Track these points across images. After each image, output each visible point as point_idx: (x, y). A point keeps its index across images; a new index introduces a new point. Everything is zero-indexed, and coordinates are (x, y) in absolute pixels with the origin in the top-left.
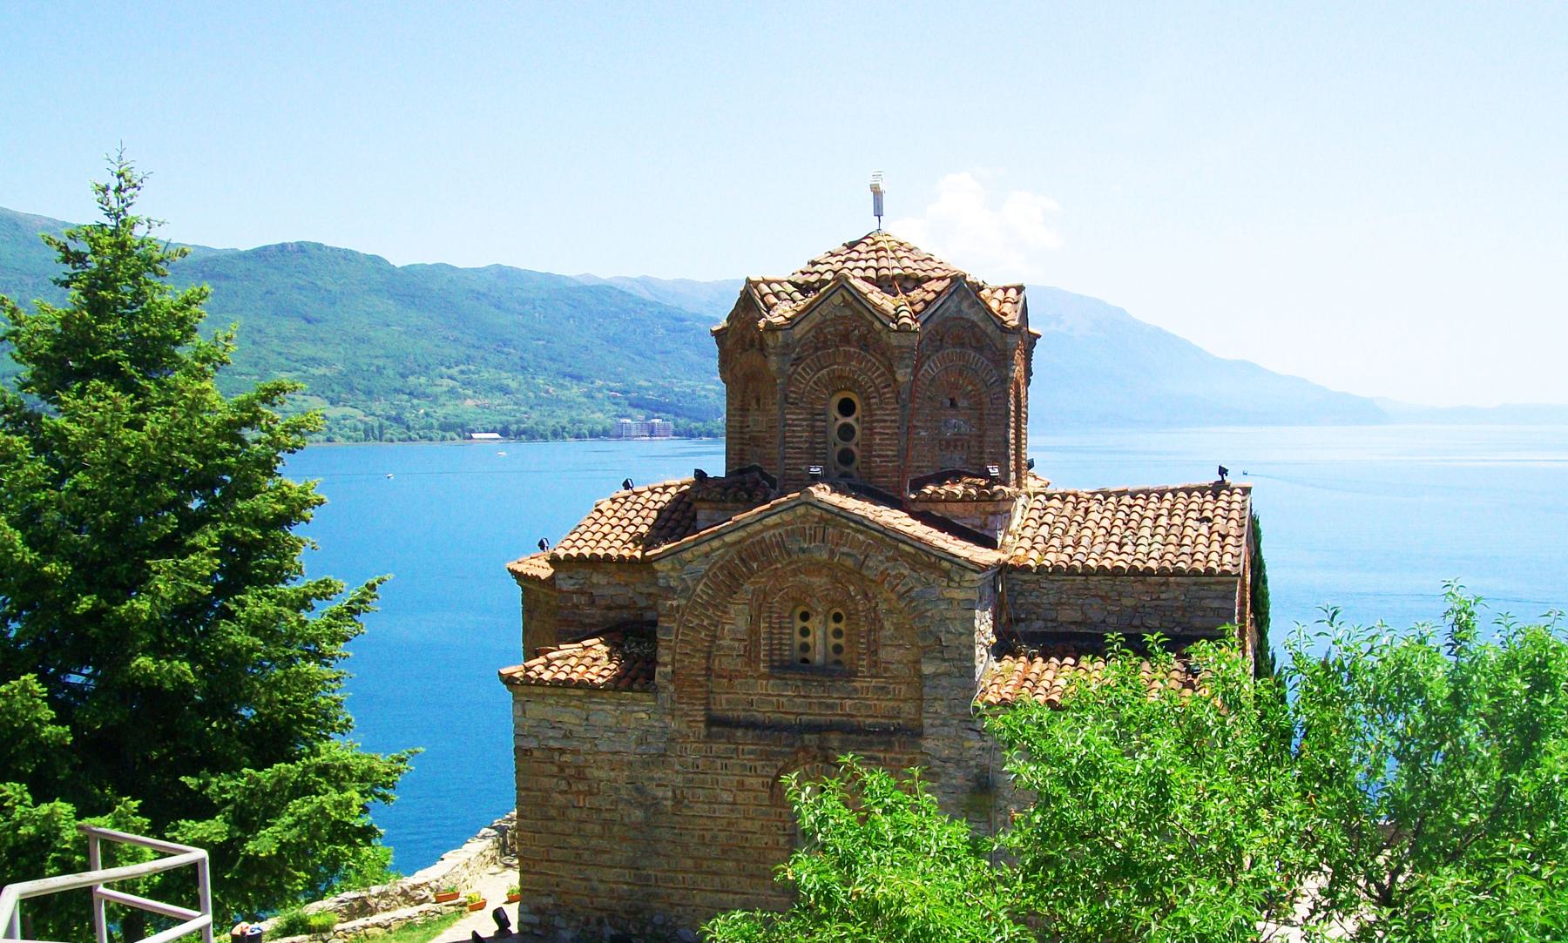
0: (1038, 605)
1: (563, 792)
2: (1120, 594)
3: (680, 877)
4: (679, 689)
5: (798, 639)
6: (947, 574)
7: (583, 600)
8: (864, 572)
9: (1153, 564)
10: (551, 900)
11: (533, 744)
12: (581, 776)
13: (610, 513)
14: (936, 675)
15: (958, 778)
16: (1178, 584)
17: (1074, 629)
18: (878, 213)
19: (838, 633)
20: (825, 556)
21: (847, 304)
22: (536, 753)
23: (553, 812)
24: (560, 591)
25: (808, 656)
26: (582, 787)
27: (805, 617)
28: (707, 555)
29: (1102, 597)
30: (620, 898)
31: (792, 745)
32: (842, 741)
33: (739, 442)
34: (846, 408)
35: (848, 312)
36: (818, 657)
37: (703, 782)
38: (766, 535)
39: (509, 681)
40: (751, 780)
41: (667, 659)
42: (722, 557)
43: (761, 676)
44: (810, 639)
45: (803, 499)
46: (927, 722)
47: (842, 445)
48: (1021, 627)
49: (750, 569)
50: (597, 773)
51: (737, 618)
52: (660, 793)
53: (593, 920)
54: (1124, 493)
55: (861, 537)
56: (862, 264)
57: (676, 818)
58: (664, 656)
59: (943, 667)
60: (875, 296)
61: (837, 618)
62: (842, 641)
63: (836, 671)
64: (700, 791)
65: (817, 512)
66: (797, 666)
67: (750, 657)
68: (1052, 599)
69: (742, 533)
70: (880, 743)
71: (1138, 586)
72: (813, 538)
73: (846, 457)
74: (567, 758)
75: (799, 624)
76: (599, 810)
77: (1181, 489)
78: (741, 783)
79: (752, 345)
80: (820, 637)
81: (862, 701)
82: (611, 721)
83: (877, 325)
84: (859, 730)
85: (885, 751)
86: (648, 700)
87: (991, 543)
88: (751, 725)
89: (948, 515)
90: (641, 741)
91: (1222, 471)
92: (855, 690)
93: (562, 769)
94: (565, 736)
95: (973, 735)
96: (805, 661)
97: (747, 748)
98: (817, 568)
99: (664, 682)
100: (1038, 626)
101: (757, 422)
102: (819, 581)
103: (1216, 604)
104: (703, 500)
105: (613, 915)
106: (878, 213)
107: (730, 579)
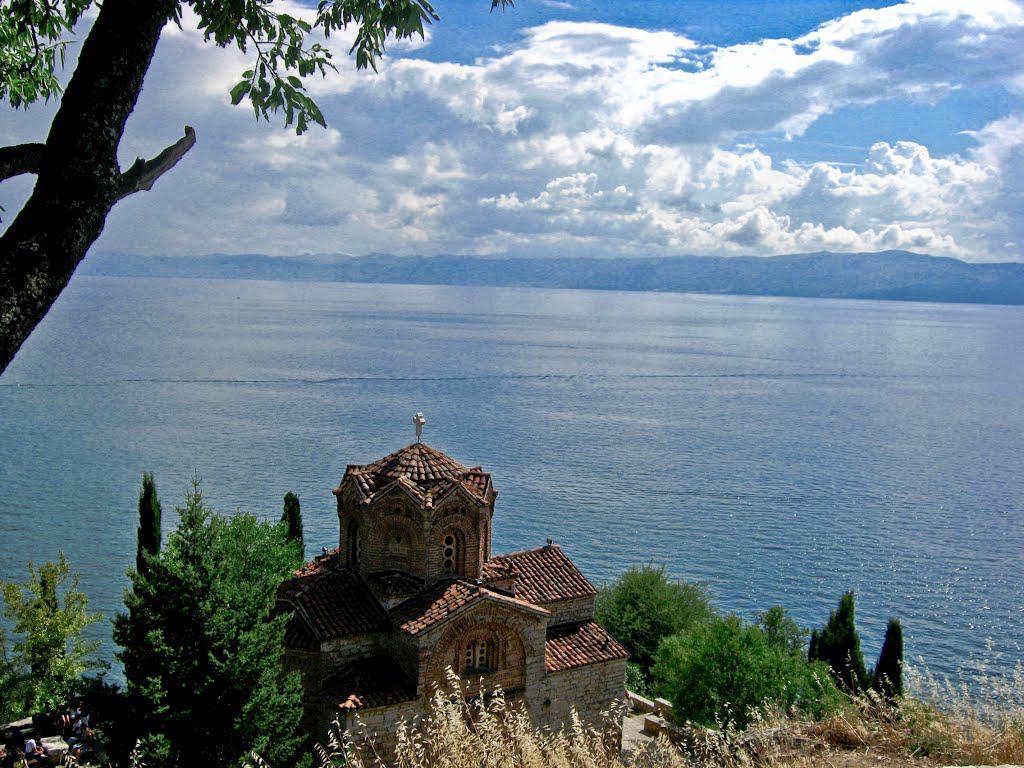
6: (538, 620)
18: (418, 433)
25: (471, 664)
27: (469, 647)
28: (441, 629)
59: (534, 659)
61: (483, 645)
83: (471, 504)
86: (415, 703)
103: (588, 607)
106: (418, 433)
107: (450, 637)
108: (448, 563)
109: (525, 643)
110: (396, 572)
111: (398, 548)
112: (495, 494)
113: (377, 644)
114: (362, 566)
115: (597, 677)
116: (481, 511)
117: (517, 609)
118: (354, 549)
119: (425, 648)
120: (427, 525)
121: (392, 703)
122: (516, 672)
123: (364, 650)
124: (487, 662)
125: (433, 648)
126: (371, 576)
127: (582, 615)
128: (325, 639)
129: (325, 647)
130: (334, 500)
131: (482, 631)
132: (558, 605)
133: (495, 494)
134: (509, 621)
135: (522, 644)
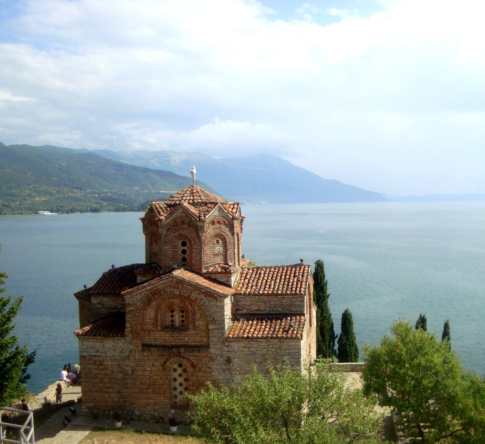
0: (245, 305)
1: (96, 369)
2: (270, 301)
3: (134, 395)
4: (133, 335)
5: (170, 319)
6: (216, 298)
7: (100, 306)
8: (191, 298)
9: (280, 292)
10: (92, 404)
11: (86, 354)
13: (107, 277)
14: (213, 329)
15: (221, 360)
16: (287, 298)
17: (256, 312)
19: (183, 316)
20: (178, 293)
21: (183, 212)
22: (87, 357)
23: (92, 376)
24: (93, 304)
25: (174, 323)
26: (102, 367)
27: (172, 311)
28: (141, 293)
29: (264, 302)
30: (115, 403)
31: (169, 352)
32: (185, 351)
33: (150, 253)
34: (184, 244)
35: (184, 215)
36: (177, 323)
37: (141, 364)
38: (160, 287)
39: (78, 335)
40: (157, 363)
41: (129, 326)
42: (145, 294)
43: (159, 331)
44: (174, 318)
45: (171, 276)
46: (211, 344)
47: (183, 256)
48: (240, 312)
49: (155, 297)
51: (150, 313)
52: (127, 368)
53: (106, 410)
54: (271, 267)
55: (189, 287)
56: (188, 198)
57: (133, 376)
58: (128, 325)
60: (192, 209)
61: (182, 312)
62: (184, 319)
64: (140, 368)
65: (175, 280)
66: (171, 328)
67: (155, 324)
68: (249, 303)
69: (152, 286)
70: (197, 351)
71: (275, 299)
72: (174, 288)
73: (184, 259)
74: (97, 358)
75: (170, 314)
76: (107, 374)
77: (290, 266)
78: (153, 365)
79: (153, 224)
80: (177, 318)
81: (190, 337)
82: (111, 346)
83: (193, 219)
85: (199, 353)
87: (229, 286)
88: (156, 346)
89: (216, 278)
90: (121, 352)
91: (302, 260)
92: (188, 334)
93: (95, 362)
94: (96, 352)
95: (226, 347)
96: (172, 325)
97: (155, 353)
98: (175, 297)
99: (128, 334)
100: (245, 311)
101: (155, 248)
102: (176, 301)
103: (299, 303)
104: (138, 274)
107: (148, 301)
109: (207, 314)
110: (154, 263)
115: (273, 350)
117: (197, 287)
119: (130, 304)
122: (204, 334)
127: (293, 309)
131: (175, 301)
134: (192, 295)
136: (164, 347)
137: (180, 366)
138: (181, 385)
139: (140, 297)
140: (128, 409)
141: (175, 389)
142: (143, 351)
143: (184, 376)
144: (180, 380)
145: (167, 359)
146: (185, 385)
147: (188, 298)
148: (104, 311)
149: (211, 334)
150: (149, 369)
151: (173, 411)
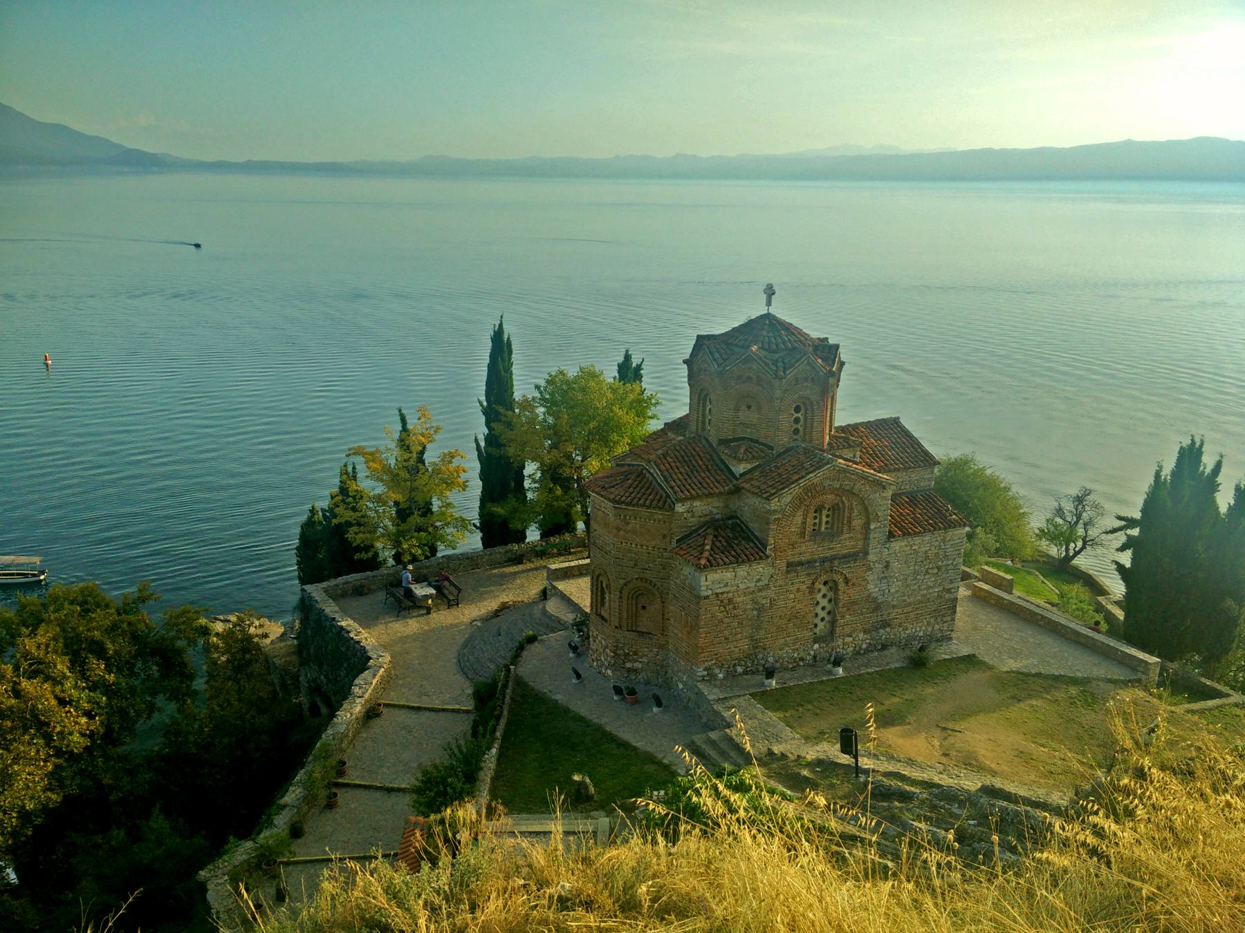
12: (730, 601)
15: (879, 567)
18: (769, 303)
21: (809, 364)
34: (797, 410)
47: (795, 426)
50: (739, 600)
58: (771, 541)
63: (833, 534)
67: (802, 534)
84: (844, 556)
88: (801, 564)
90: (759, 580)
98: (833, 491)
105: (739, 660)
106: (769, 303)
108: (796, 431)
109: (870, 510)
110: (743, 439)
111: (744, 415)
112: (842, 364)
113: (727, 506)
114: (713, 432)
116: (831, 380)
118: (704, 416)
119: (775, 511)
120: (778, 393)
121: (743, 561)
123: (715, 511)
124: (832, 528)
125: (783, 511)
126: (721, 442)
128: (678, 500)
129: (680, 508)
130: (684, 370)
132: (899, 474)
133: (842, 364)
135: (866, 510)
136: (810, 563)
137: (825, 583)
138: (823, 608)
139: (789, 499)
140: (760, 656)
141: (817, 615)
142: (787, 572)
143: (831, 595)
144: (824, 602)
145: (816, 579)
146: (829, 607)
147: (851, 493)
148: (693, 521)
149: (872, 536)
150: (792, 596)
151: (816, 646)
